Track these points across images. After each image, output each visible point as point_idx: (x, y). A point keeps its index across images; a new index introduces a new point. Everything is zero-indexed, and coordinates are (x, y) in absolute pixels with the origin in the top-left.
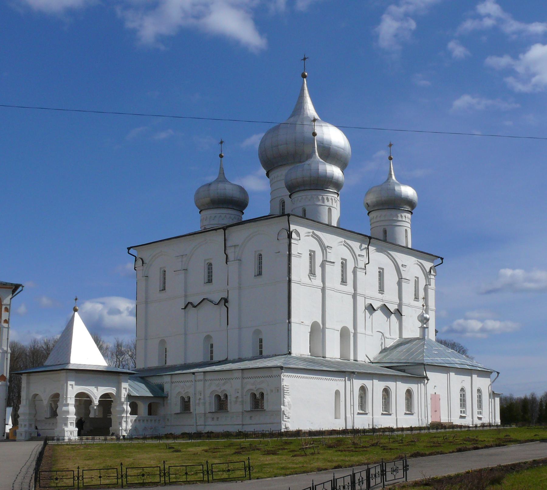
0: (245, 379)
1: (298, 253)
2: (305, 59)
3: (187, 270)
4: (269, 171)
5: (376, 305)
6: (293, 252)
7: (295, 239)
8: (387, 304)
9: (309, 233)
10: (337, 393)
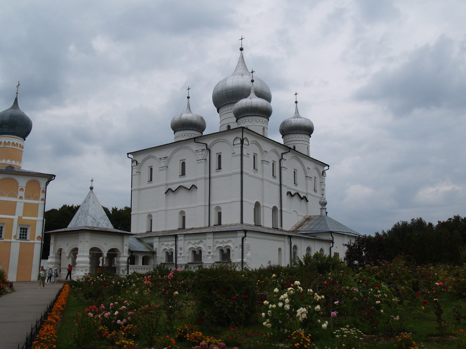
0: (215, 239)
1: (247, 154)
2: (242, 39)
4: (219, 108)
5: (293, 193)
6: (245, 153)
7: (246, 145)
8: (299, 193)
9: (254, 141)
10: (280, 249)
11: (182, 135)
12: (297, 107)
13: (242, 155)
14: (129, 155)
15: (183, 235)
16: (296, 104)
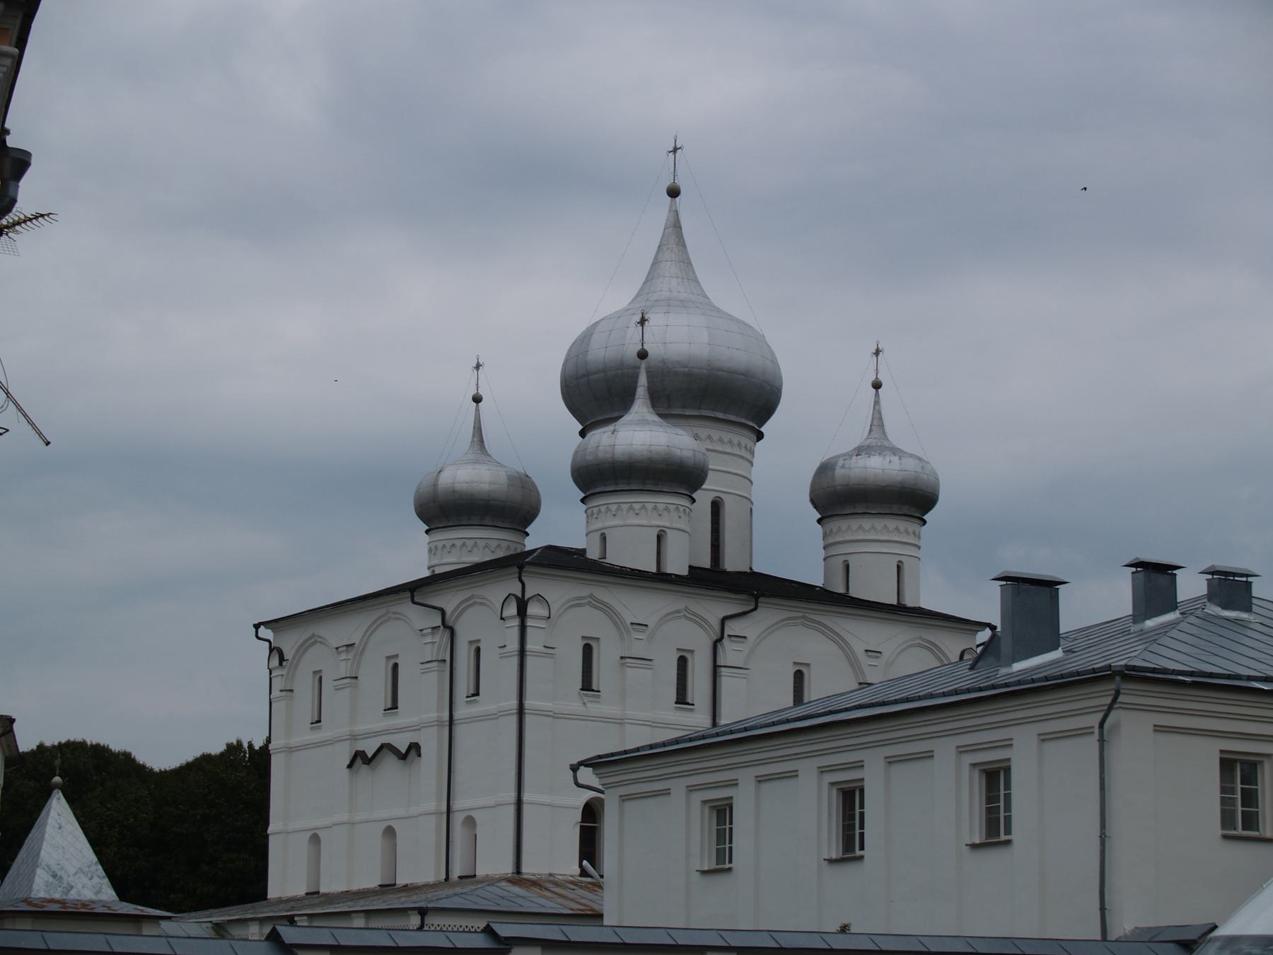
1: (545, 646)
2: (675, 150)
3: (356, 678)
11: (454, 545)
12: (877, 402)
13: (522, 653)
14: (260, 630)
15: (305, 918)
16: (877, 392)
